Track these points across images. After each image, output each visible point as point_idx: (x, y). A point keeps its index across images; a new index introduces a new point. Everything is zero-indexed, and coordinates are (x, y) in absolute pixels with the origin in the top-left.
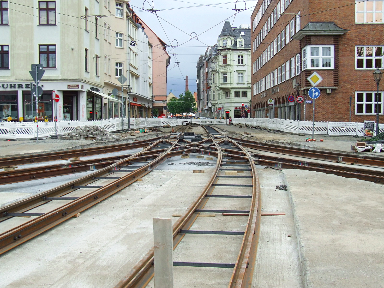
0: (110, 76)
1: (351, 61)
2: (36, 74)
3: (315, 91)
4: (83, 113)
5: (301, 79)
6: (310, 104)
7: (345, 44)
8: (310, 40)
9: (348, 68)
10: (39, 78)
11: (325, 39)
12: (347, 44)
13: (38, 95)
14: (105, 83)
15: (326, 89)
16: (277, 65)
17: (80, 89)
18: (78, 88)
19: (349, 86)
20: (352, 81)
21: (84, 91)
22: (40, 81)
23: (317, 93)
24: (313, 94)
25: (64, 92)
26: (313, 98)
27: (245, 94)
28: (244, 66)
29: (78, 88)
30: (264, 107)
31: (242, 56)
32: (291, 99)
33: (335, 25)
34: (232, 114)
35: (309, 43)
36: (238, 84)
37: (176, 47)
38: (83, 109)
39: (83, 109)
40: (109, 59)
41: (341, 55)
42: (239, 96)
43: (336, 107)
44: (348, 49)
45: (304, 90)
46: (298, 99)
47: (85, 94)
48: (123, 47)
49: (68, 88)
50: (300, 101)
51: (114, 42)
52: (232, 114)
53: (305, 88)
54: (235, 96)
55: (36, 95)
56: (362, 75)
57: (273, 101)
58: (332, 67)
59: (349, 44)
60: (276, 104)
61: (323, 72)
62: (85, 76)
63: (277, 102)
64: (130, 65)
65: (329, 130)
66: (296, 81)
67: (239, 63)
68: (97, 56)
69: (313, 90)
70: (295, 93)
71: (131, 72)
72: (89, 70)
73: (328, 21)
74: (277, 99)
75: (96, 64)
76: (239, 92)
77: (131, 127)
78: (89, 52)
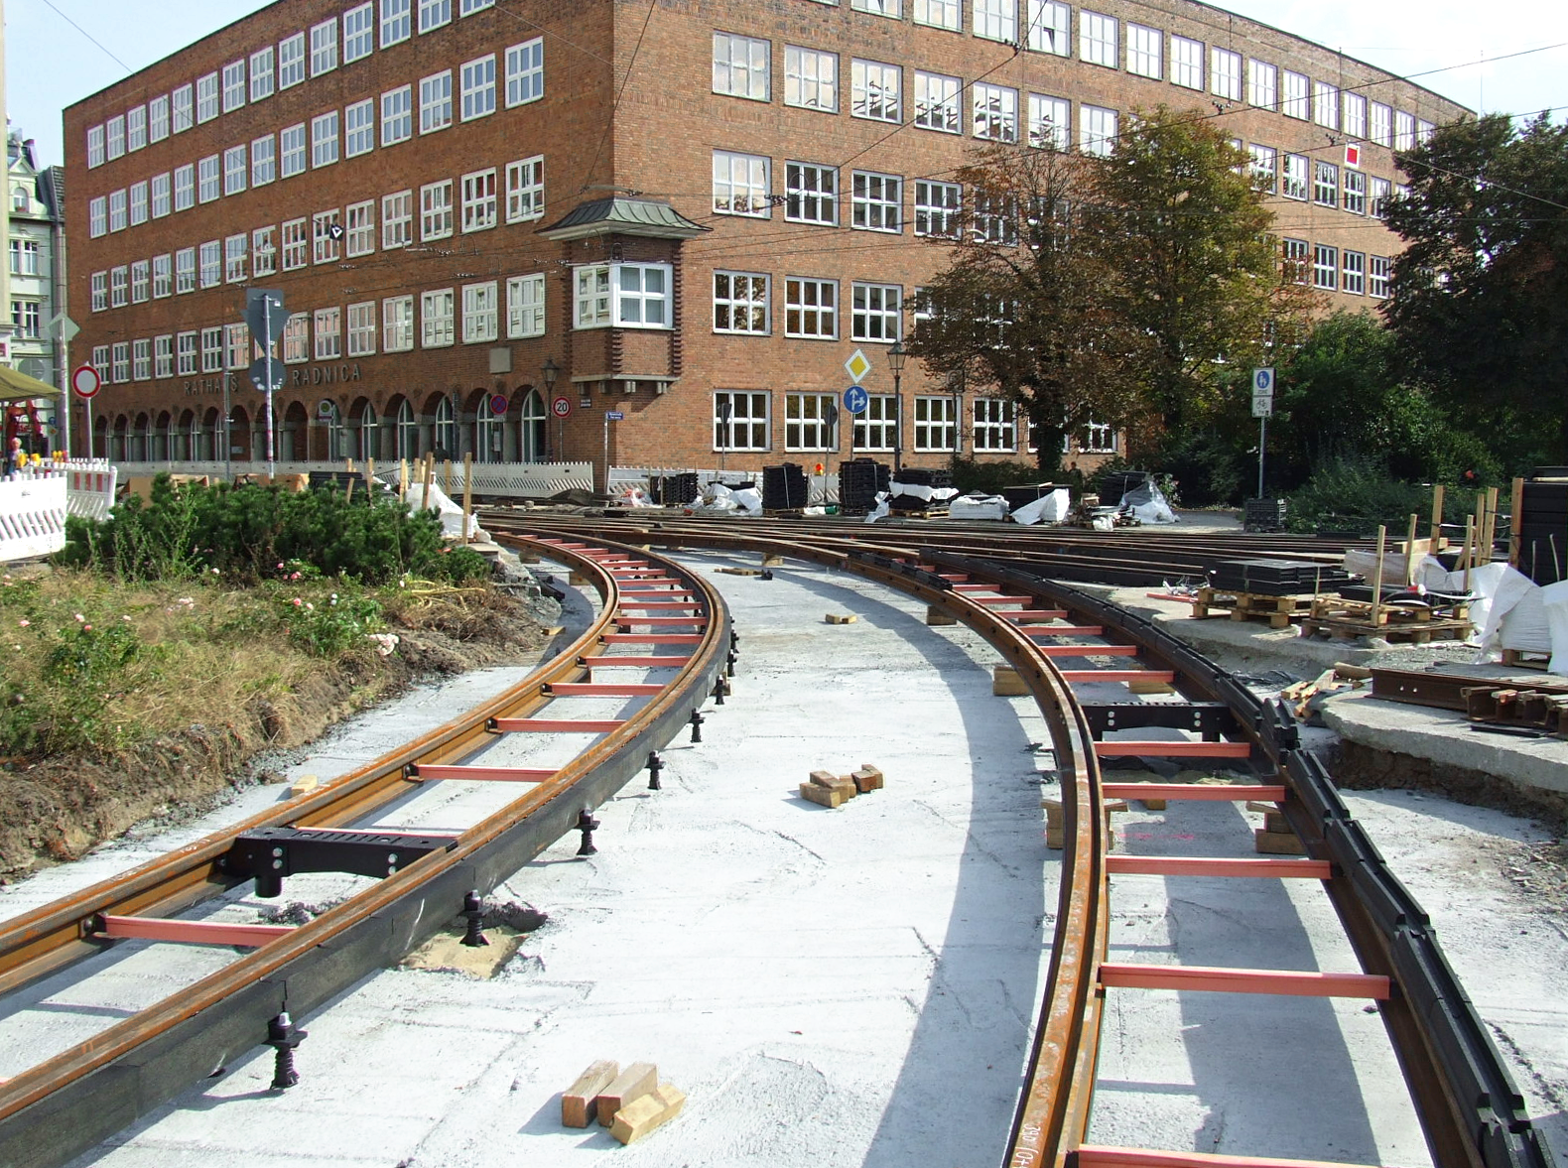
15: (654, 383)
24: (854, 403)
41: (685, 290)
43: (676, 430)
46: (557, 407)
50: (562, 413)
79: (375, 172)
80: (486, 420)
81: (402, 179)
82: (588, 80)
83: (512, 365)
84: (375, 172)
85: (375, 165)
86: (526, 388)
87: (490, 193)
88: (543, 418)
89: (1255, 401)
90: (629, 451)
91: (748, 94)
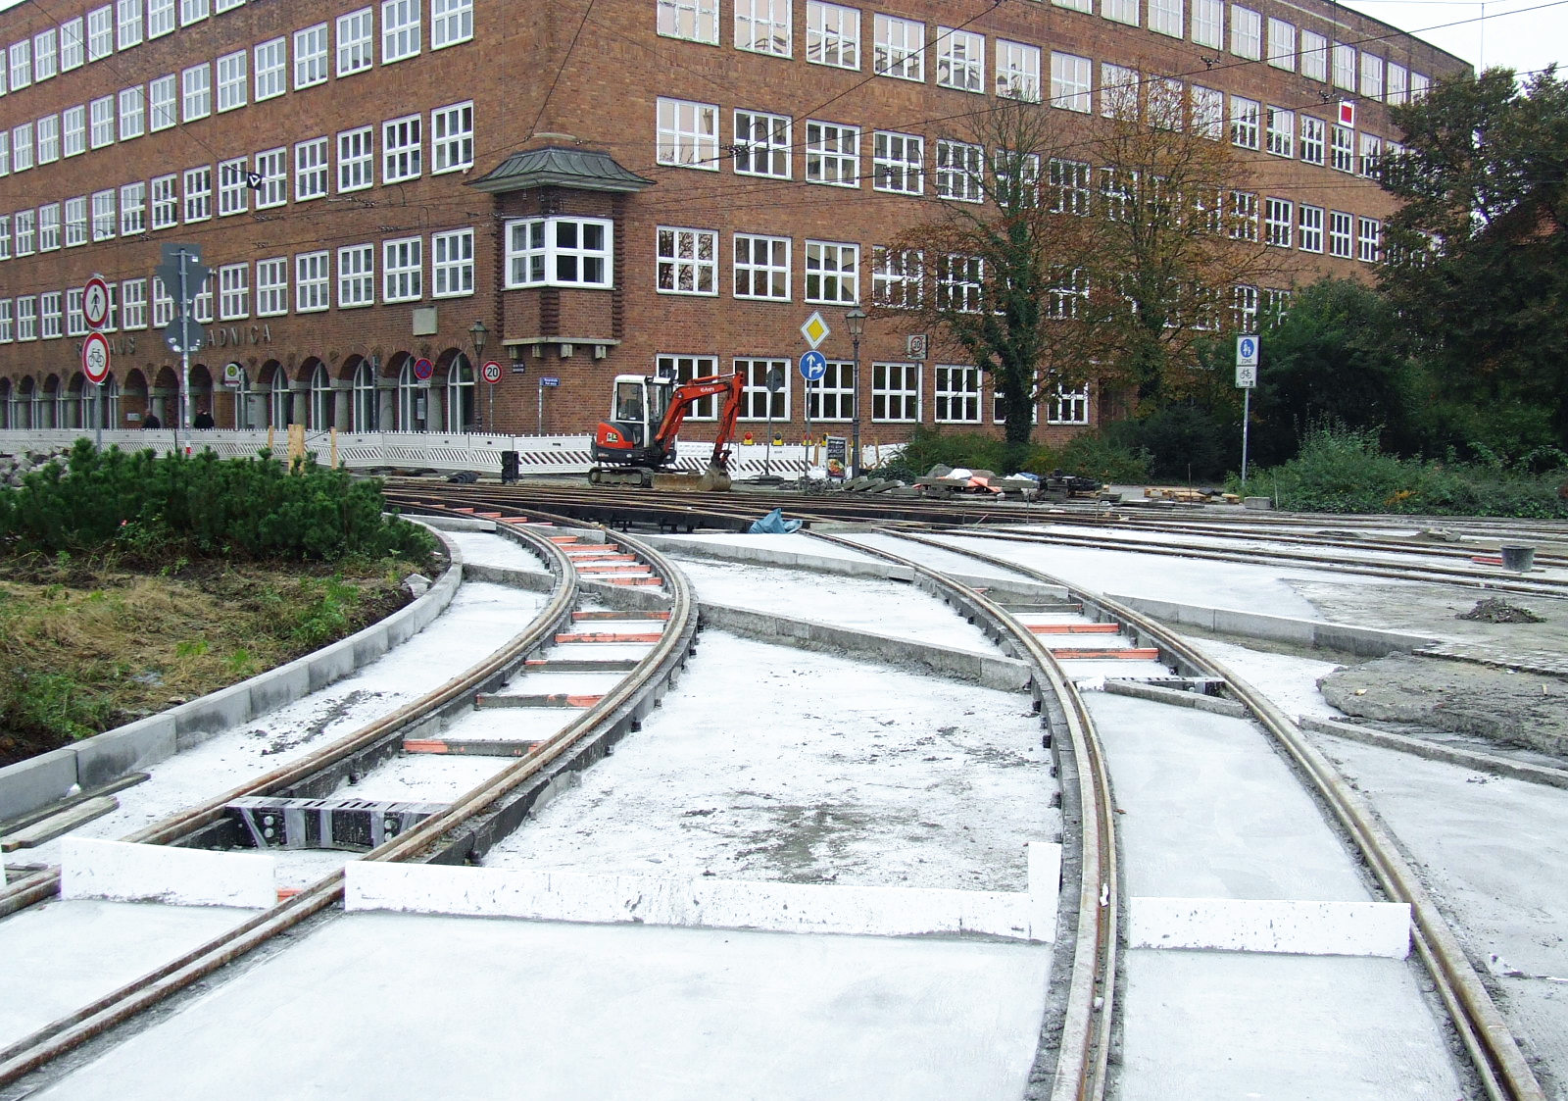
2: (180, 276)
6: (552, 388)
9: (640, 289)
15: (592, 347)
19: (642, 338)
23: (819, 365)
24: (811, 369)
32: (424, 369)
41: (627, 246)
46: (487, 372)
50: (493, 378)
56: (672, 309)
57: (238, 373)
58: (608, 282)
59: (643, 220)
61: (588, 296)
69: (811, 358)
79: (287, 117)
80: (409, 385)
81: (317, 125)
82: (522, 20)
83: (439, 326)
84: (287, 117)
85: (287, 109)
86: (454, 351)
87: (415, 140)
88: (472, 383)
89: (1239, 371)
90: (565, 419)
91: (694, 36)
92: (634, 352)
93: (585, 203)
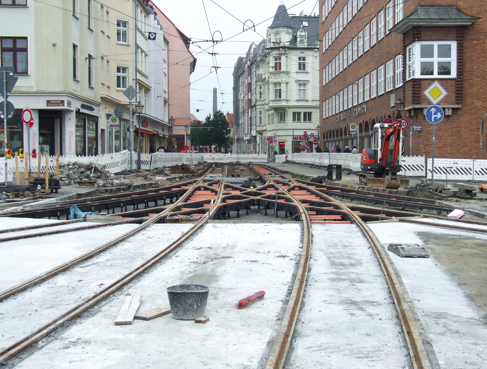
0: (108, 87)
1: (482, 66)
3: (435, 111)
4: (70, 144)
5: (404, 94)
6: (419, 131)
7: (473, 40)
8: (420, 34)
9: (477, 77)
10: (9, 89)
11: (443, 32)
12: (476, 40)
13: (7, 116)
14: (102, 98)
16: (364, 72)
17: (66, 107)
18: (64, 106)
19: (479, 104)
20: (483, 96)
21: (72, 111)
22: (10, 93)
23: (439, 114)
24: (433, 116)
25: (41, 112)
26: (432, 122)
27: (308, 117)
28: (307, 73)
29: (64, 106)
30: (341, 135)
31: (304, 59)
33: (458, 10)
34: (288, 147)
35: (418, 38)
36: (297, 101)
37: (218, 42)
38: (70, 138)
39: (70, 138)
40: (108, 62)
41: (467, 56)
42: (299, 119)
44: (477, 47)
45: (409, 111)
47: (73, 115)
48: (128, 44)
49: (47, 106)
51: (114, 36)
52: (288, 147)
53: (410, 107)
54: (294, 119)
55: (4, 115)
58: (454, 74)
59: (479, 40)
60: (361, 131)
62: (73, 87)
63: (363, 129)
64: (137, 70)
65: (474, 172)
66: (396, 97)
67: (300, 69)
68: (90, 57)
69: (433, 110)
70: (394, 114)
71: (138, 82)
72: (78, 78)
73: (447, 4)
74: (363, 123)
75: (89, 68)
76: (299, 114)
77: (143, 167)
78: (78, 50)
90: (427, 148)
92: (473, 111)
93: (438, 34)
